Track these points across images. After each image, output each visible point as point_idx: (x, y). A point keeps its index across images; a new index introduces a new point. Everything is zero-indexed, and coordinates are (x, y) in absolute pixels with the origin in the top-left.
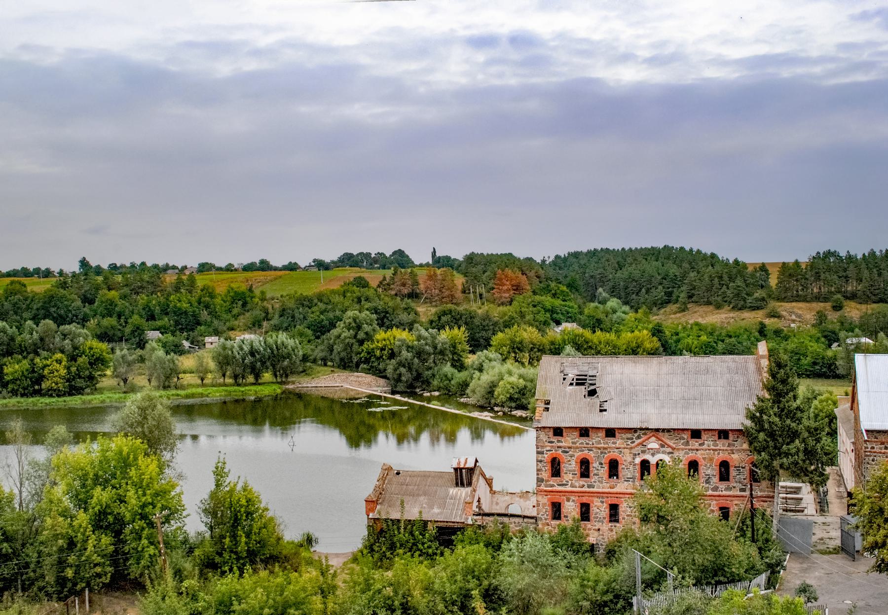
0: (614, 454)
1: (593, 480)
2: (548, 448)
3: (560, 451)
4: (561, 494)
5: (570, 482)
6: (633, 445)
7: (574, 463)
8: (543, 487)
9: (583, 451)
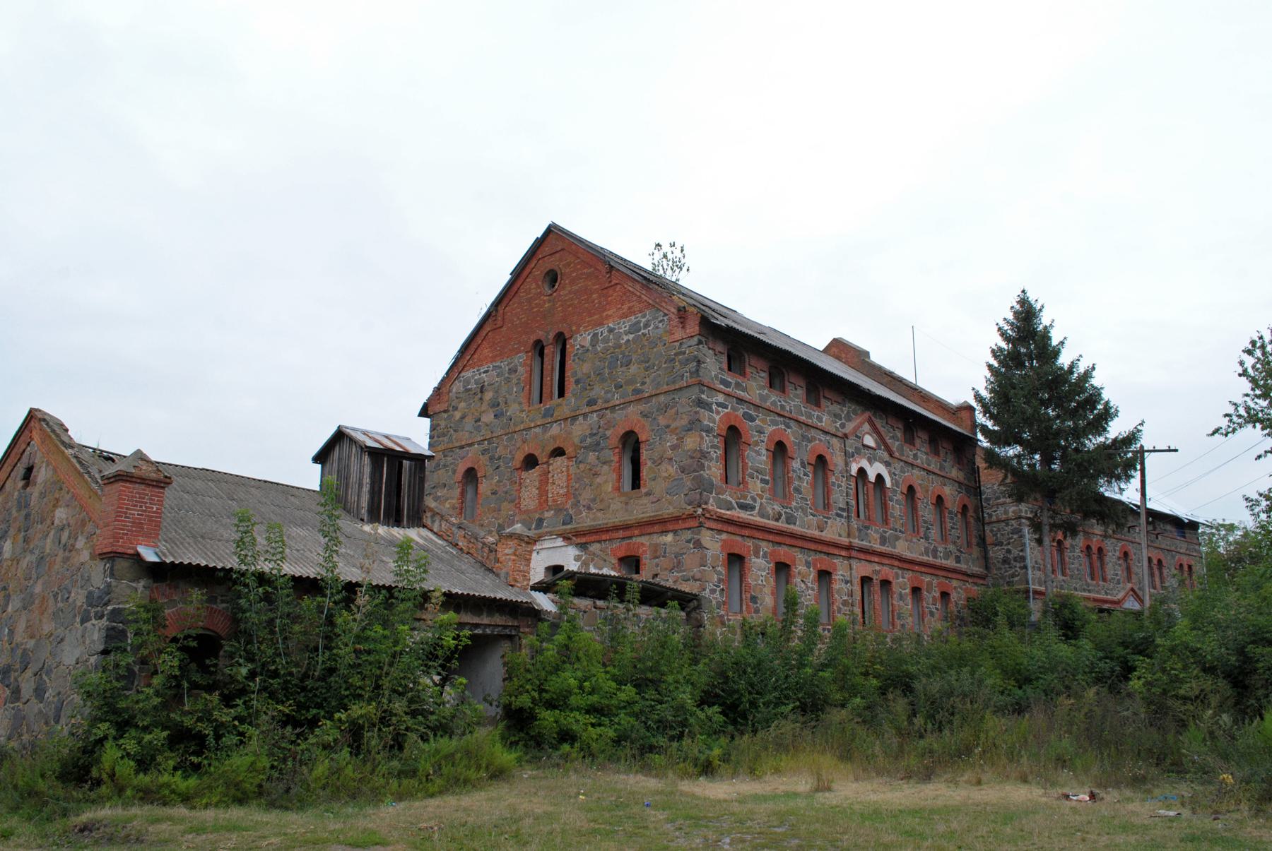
0: (819, 443)
1: (794, 504)
2: (721, 398)
3: (740, 413)
4: (747, 532)
5: (759, 501)
6: (847, 430)
7: (764, 452)
8: (712, 505)
9: (774, 423)
